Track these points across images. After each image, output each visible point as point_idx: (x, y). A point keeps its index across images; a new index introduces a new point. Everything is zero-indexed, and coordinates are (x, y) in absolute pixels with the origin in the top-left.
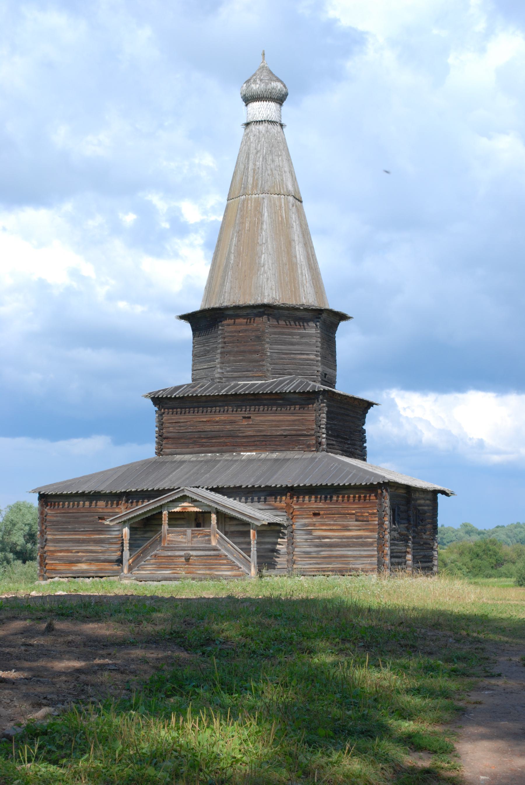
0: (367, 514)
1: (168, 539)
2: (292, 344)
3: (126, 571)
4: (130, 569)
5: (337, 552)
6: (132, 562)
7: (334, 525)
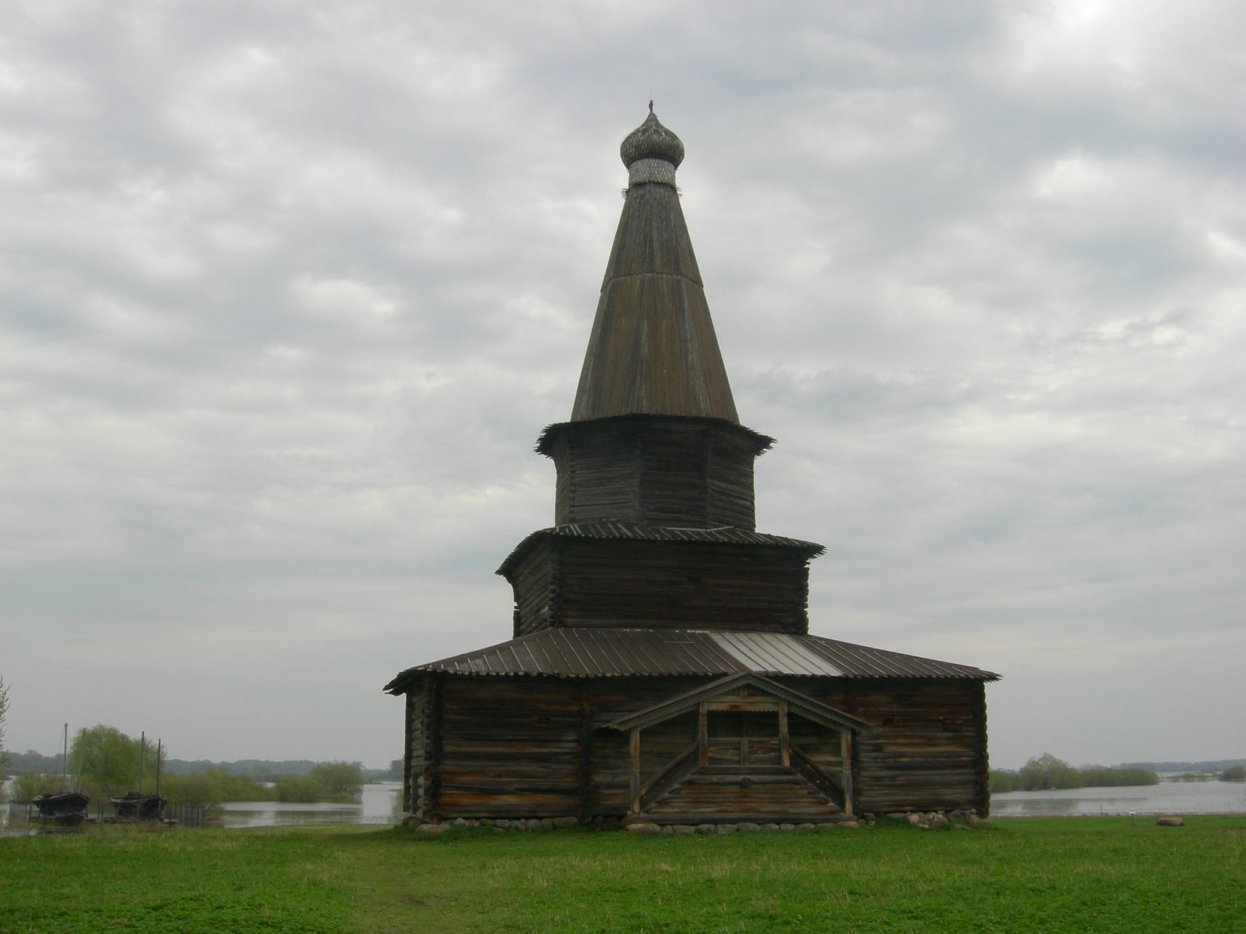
0: (960, 722)
1: (710, 755)
2: (732, 483)
3: (637, 808)
4: (643, 804)
5: (920, 775)
6: (647, 793)
7: (914, 737)
